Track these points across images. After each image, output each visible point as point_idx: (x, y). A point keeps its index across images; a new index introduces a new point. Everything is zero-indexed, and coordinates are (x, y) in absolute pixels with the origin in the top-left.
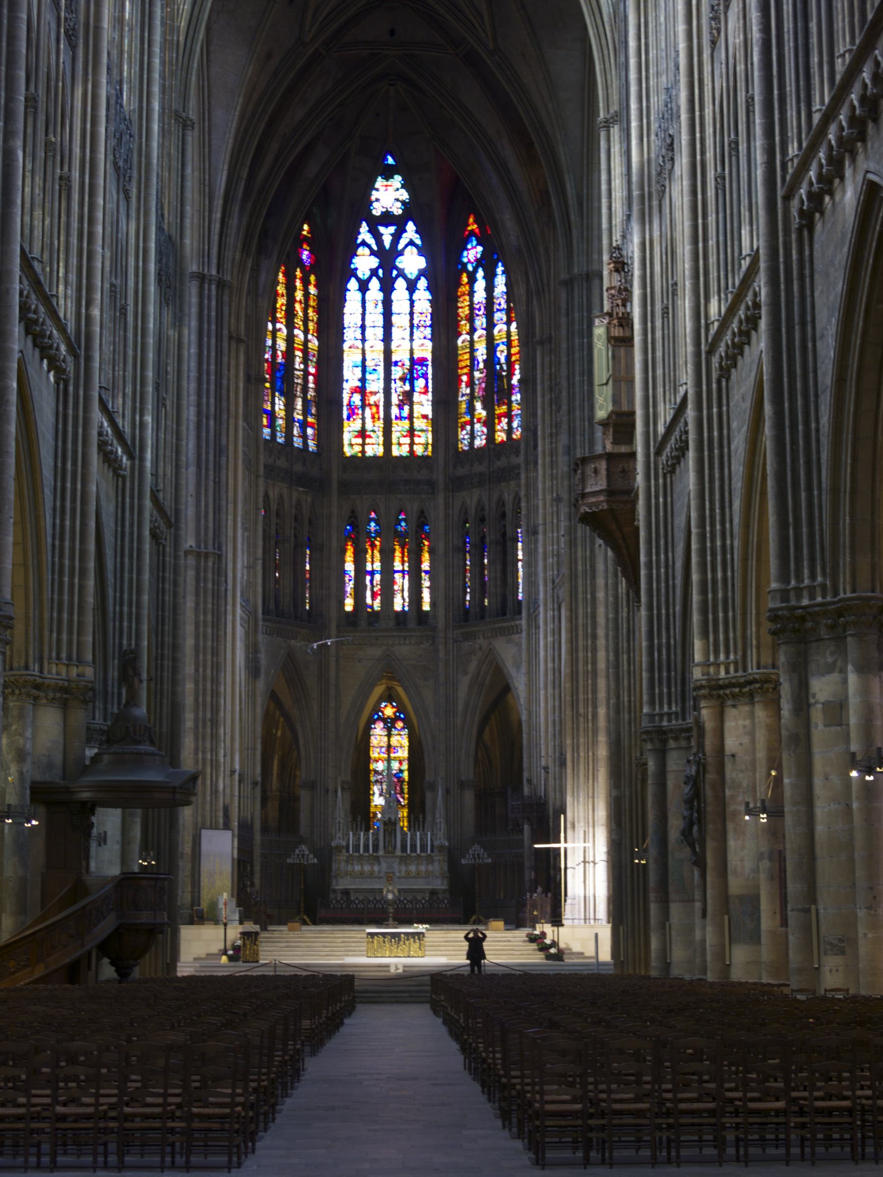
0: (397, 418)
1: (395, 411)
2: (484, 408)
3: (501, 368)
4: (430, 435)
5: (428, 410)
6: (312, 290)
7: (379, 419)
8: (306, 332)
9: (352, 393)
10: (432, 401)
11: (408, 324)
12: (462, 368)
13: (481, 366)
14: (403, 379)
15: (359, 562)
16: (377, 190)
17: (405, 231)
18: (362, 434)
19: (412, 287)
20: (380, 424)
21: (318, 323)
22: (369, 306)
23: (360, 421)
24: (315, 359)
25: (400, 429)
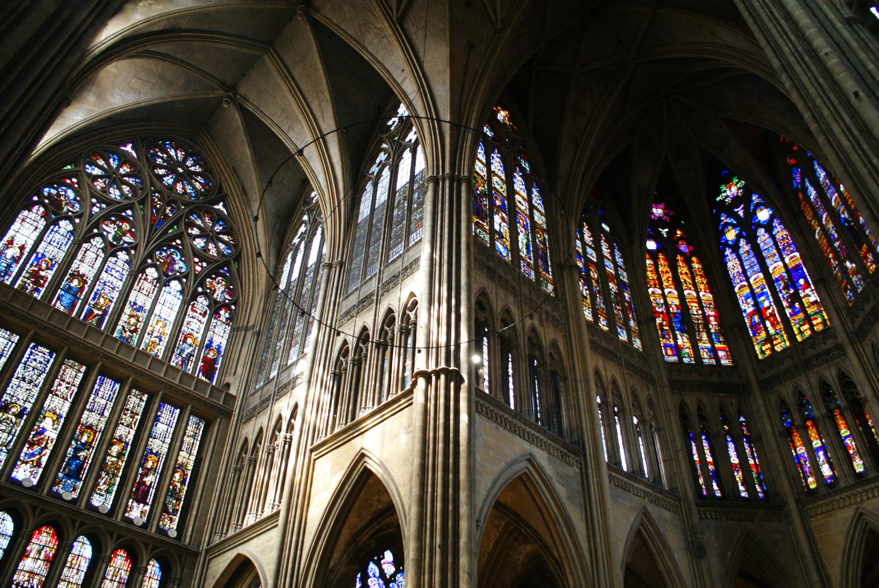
0: (791, 315)
1: (788, 311)
2: (851, 263)
3: (849, 222)
4: (824, 314)
5: (814, 297)
6: (696, 266)
7: (778, 323)
8: (697, 291)
9: (751, 317)
10: (815, 290)
11: (775, 251)
12: (826, 251)
13: (836, 236)
14: (786, 287)
15: (808, 443)
16: (725, 192)
17: (752, 201)
18: (769, 339)
19: (769, 227)
20: (780, 326)
21: (708, 283)
22: (744, 257)
23: (764, 332)
24: (712, 306)
25: (797, 321)
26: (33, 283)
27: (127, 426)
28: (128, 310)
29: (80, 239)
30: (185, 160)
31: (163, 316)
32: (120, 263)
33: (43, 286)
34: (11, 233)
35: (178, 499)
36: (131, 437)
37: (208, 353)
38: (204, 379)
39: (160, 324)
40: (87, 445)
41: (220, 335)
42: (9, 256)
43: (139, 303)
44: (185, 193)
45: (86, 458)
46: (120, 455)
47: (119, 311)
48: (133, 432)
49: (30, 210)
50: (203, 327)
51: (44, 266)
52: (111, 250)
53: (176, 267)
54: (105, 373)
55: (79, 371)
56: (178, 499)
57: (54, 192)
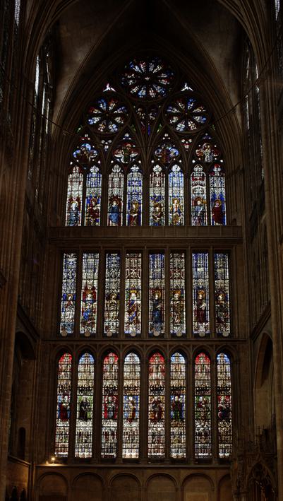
26: (93, 217)
27: (179, 278)
28: (152, 204)
29: (105, 172)
30: (147, 68)
31: (175, 195)
32: (135, 174)
33: (98, 216)
34: (69, 193)
35: (226, 312)
36: (183, 284)
37: (215, 205)
38: (217, 224)
39: (176, 201)
40: (160, 300)
41: (219, 188)
42: (74, 209)
43: (157, 195)
44: (157, 94)
45: (161, 308)
46: (180, 298)
47: (147, 206)
48: (183, 281)
49: (72, 173)
50: (205, 188)
51: (93, 203)
52: (126, 170)
53: (172, 155)
54: (153, 252)
55: (138, 258)
56: (226, 312)
57: (79, 152)
